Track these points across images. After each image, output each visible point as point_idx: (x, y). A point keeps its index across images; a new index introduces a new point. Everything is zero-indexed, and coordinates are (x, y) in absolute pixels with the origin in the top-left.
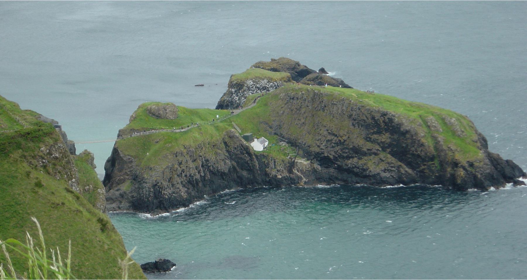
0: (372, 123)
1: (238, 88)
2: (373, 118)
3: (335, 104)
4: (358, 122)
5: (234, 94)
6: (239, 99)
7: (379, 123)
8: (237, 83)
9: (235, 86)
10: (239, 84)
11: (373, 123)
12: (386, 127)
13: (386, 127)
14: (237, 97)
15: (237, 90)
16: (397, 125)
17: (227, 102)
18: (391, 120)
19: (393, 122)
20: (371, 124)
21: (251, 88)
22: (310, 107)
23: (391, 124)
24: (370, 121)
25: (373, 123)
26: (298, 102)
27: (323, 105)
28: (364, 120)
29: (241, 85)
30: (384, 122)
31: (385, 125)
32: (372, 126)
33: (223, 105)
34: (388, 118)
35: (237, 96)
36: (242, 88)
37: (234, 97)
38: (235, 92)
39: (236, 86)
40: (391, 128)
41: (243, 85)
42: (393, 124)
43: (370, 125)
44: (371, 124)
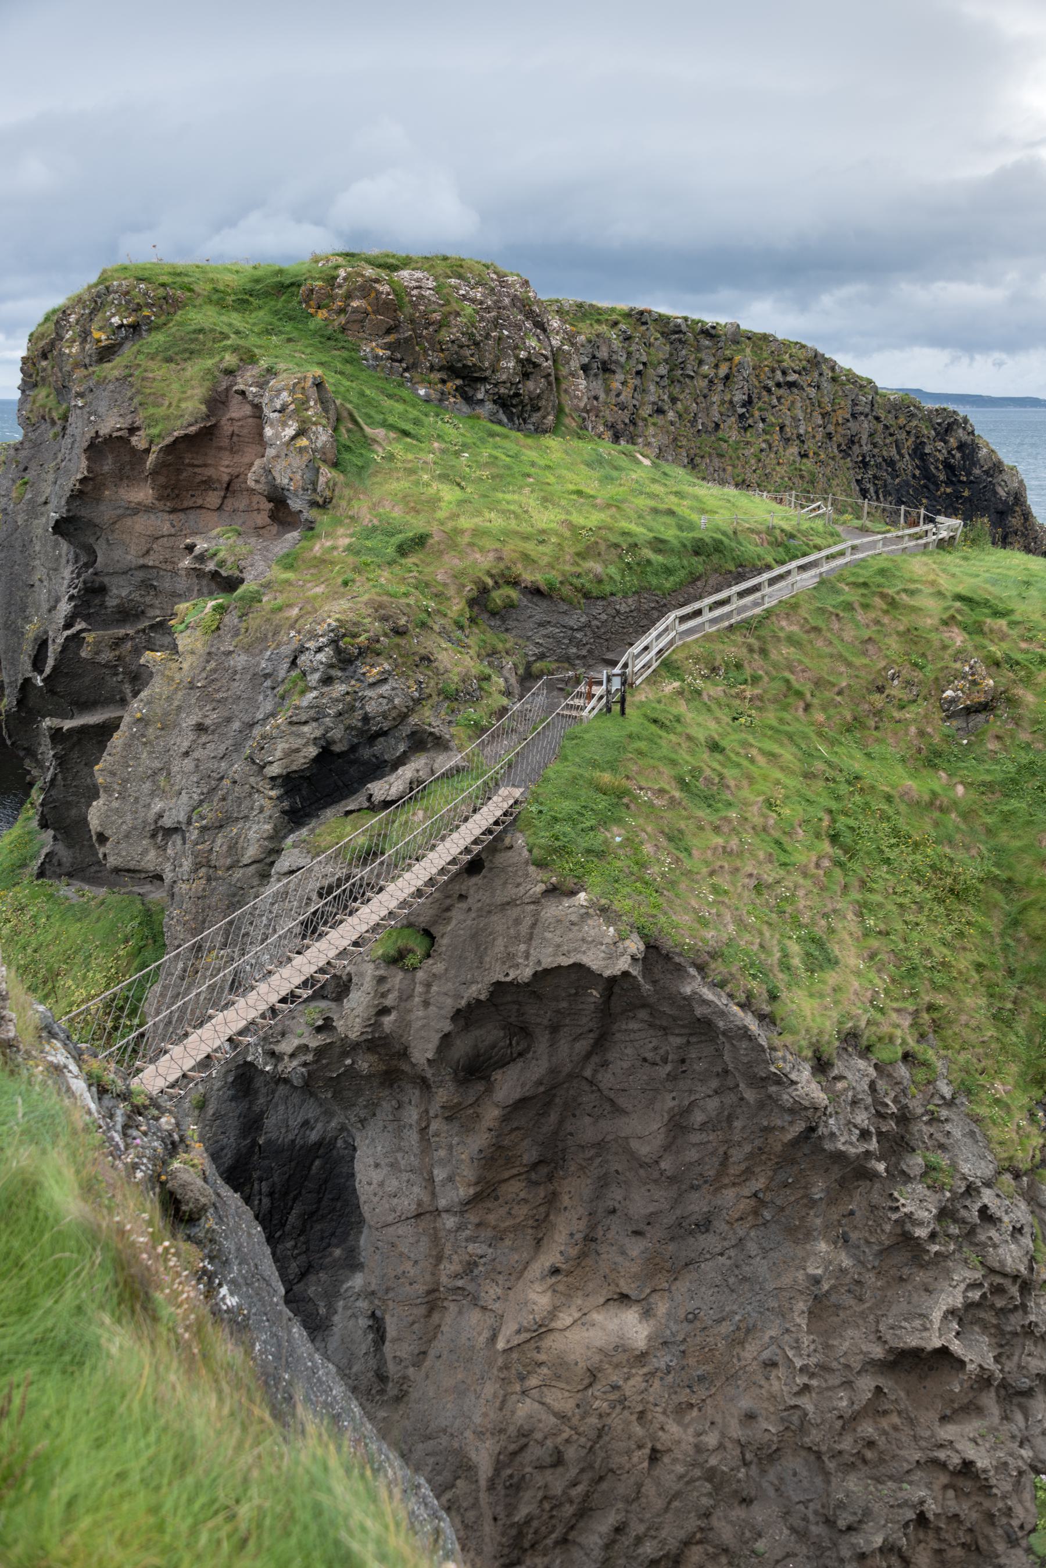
0: (914, 476)
2: (918, 452)
3: (791, 385)
4: (875, 477)
7: (932, 467)
11: (917, 472)
12: (949, 490)
13: (949, 490)
16: (986, 472)
18: (969, 449)
19: (974, 463)
20: (912, 482)
22: (671, 415)
23: (969, 474)
24: (907, 465)
25: (917, 472)
26: (616, 385)
27: (739, 397)
28: (891, 463)
30: (948, 466)
31: (949, 482)
32: (915, 490)
34: (961, 446)
40: (966, 494)
42: (977, 471)
43: (907, 483)
44: (912, 482)
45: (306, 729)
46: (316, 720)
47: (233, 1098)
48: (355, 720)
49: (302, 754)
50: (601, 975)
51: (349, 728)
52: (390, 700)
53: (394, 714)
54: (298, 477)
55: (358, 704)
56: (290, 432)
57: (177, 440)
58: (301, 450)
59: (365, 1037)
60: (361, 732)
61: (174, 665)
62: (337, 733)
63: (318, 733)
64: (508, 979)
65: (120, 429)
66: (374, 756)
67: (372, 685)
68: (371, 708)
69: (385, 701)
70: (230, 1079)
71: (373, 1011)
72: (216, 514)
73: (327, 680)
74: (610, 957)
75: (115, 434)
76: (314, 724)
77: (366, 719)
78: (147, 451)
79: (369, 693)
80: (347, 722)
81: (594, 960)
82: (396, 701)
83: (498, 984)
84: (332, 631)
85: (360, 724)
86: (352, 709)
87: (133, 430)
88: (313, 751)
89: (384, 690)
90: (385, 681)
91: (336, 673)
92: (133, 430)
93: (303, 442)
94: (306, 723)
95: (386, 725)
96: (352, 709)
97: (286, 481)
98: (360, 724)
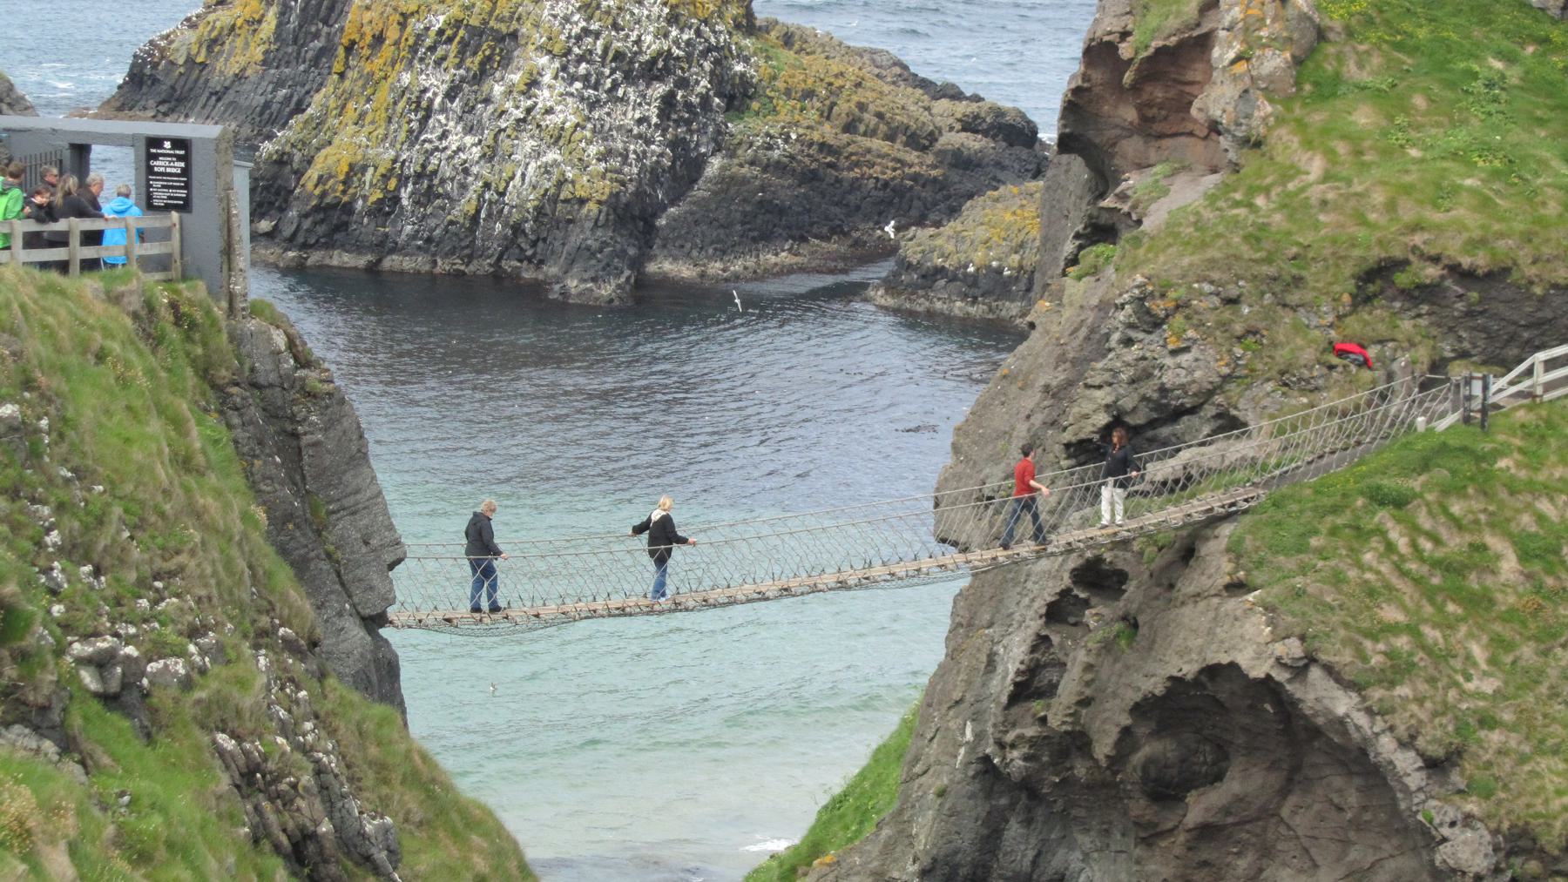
1: (473, 63)
5: (443, 110)
6: (489, 156)
8: (458, 24)
9: (440, 52)
10: (478, 33)
14: (469, 140)
15: (463, 80)
17: (386, 177)
21: (580, 59)
29: (500, 38)
33: (348, 208)
35: (469, 130)
36: (506, 62)
37: (444, 136)
38: (451, 95)
39: (453, 48)
41: (514, 35)
45: (1098, 393)
46: (1110, 385)
47: (972, 796)
48: (1149, 389)
49: (1090, 421)
50: (1247, 676)
51: (1144, 398)
52: (1190, 371)
53: (1194, 388)
54: (1230, 108)
55: (1156, 372)
56: (1231, 55)
57: (1158, 51)
58: (1235, 78)
59: (1064, 728)
60: (1158, 407)
61: (1055, 318)
62: (1127, 403)
63: (1109, 400)
64: (1180, 674)
65: (1110, 33)
66: (1175, 435)
67: (1174, 353)
68: (1168, 379)
69: (1183, 372)
70: (971, 773)
71: (1074, 699)
72: (1203, 143)
73: (1128, 342)
74: (1258, 656)
75: (1106, 38)
76: (1107, 389)
77: (1163, 390)
78: (1131, 60)
79: (1169, 361)
80: (1142, 391)
81: (1244, 659)
82: (1198, 374)
83: (1171, 678)
84: (1138, 287)
85: (1155, 396)
86: (1149, 376)
87: (1125, 35)
88: (1103, 419)
89: (1185, 359)
90: (1187, 350)
91: (1133, 334)
92: (1125, 35)
93: (1241, 67)
94: (1100, 387)
95: (1188, 402)
96: (1149, 376)
97: (1219, 113)
98: (1155, 396)
